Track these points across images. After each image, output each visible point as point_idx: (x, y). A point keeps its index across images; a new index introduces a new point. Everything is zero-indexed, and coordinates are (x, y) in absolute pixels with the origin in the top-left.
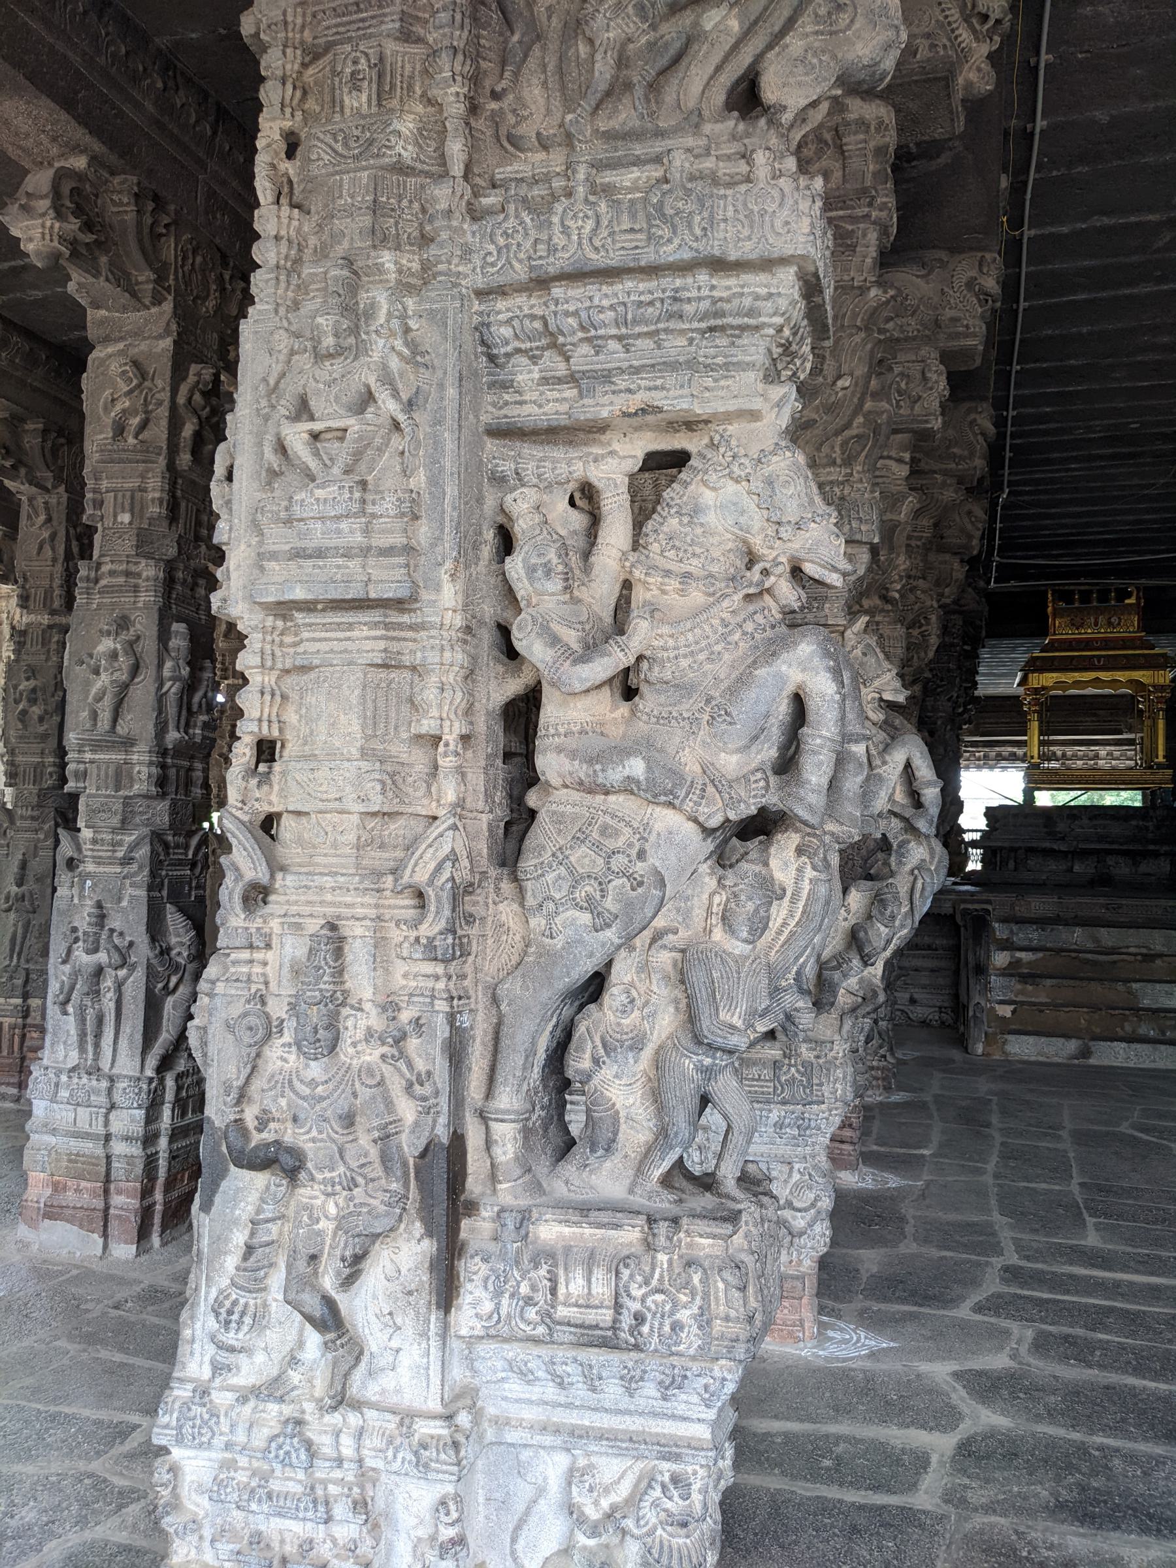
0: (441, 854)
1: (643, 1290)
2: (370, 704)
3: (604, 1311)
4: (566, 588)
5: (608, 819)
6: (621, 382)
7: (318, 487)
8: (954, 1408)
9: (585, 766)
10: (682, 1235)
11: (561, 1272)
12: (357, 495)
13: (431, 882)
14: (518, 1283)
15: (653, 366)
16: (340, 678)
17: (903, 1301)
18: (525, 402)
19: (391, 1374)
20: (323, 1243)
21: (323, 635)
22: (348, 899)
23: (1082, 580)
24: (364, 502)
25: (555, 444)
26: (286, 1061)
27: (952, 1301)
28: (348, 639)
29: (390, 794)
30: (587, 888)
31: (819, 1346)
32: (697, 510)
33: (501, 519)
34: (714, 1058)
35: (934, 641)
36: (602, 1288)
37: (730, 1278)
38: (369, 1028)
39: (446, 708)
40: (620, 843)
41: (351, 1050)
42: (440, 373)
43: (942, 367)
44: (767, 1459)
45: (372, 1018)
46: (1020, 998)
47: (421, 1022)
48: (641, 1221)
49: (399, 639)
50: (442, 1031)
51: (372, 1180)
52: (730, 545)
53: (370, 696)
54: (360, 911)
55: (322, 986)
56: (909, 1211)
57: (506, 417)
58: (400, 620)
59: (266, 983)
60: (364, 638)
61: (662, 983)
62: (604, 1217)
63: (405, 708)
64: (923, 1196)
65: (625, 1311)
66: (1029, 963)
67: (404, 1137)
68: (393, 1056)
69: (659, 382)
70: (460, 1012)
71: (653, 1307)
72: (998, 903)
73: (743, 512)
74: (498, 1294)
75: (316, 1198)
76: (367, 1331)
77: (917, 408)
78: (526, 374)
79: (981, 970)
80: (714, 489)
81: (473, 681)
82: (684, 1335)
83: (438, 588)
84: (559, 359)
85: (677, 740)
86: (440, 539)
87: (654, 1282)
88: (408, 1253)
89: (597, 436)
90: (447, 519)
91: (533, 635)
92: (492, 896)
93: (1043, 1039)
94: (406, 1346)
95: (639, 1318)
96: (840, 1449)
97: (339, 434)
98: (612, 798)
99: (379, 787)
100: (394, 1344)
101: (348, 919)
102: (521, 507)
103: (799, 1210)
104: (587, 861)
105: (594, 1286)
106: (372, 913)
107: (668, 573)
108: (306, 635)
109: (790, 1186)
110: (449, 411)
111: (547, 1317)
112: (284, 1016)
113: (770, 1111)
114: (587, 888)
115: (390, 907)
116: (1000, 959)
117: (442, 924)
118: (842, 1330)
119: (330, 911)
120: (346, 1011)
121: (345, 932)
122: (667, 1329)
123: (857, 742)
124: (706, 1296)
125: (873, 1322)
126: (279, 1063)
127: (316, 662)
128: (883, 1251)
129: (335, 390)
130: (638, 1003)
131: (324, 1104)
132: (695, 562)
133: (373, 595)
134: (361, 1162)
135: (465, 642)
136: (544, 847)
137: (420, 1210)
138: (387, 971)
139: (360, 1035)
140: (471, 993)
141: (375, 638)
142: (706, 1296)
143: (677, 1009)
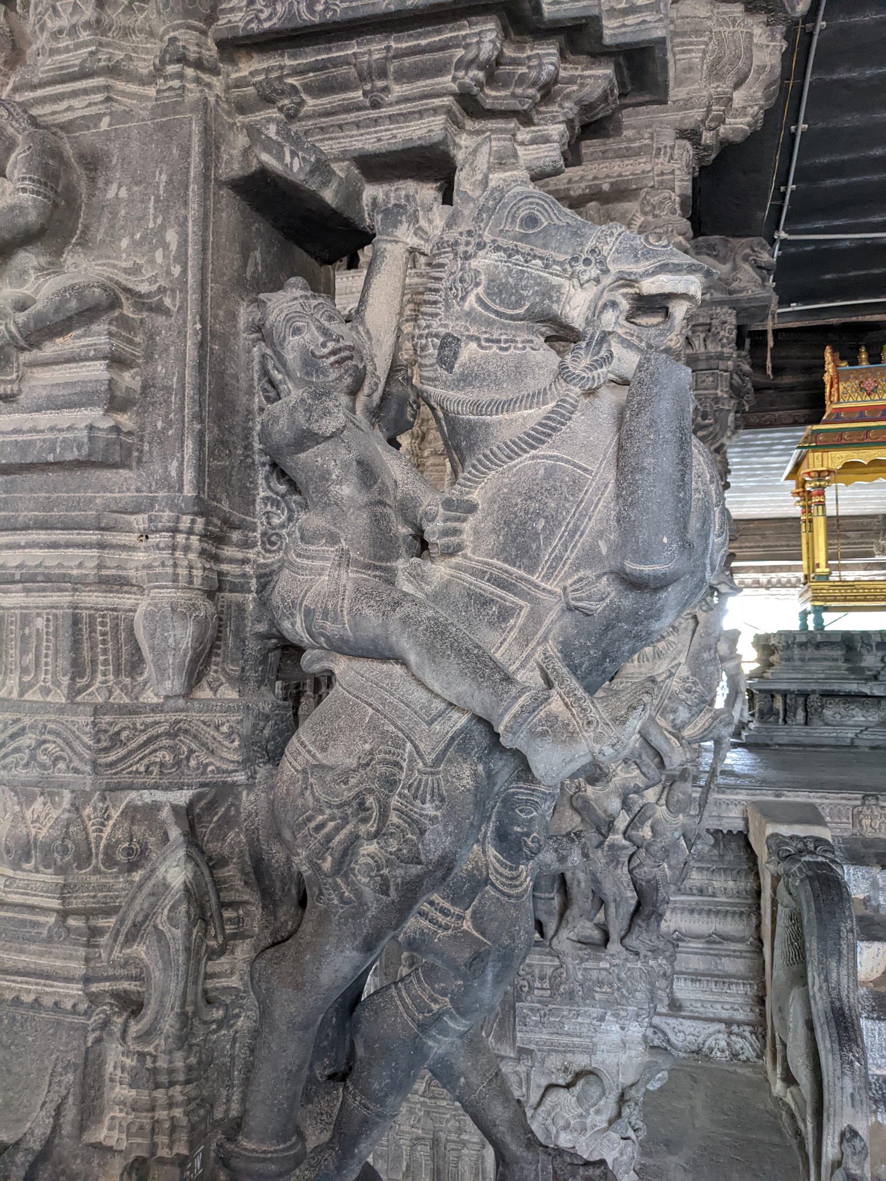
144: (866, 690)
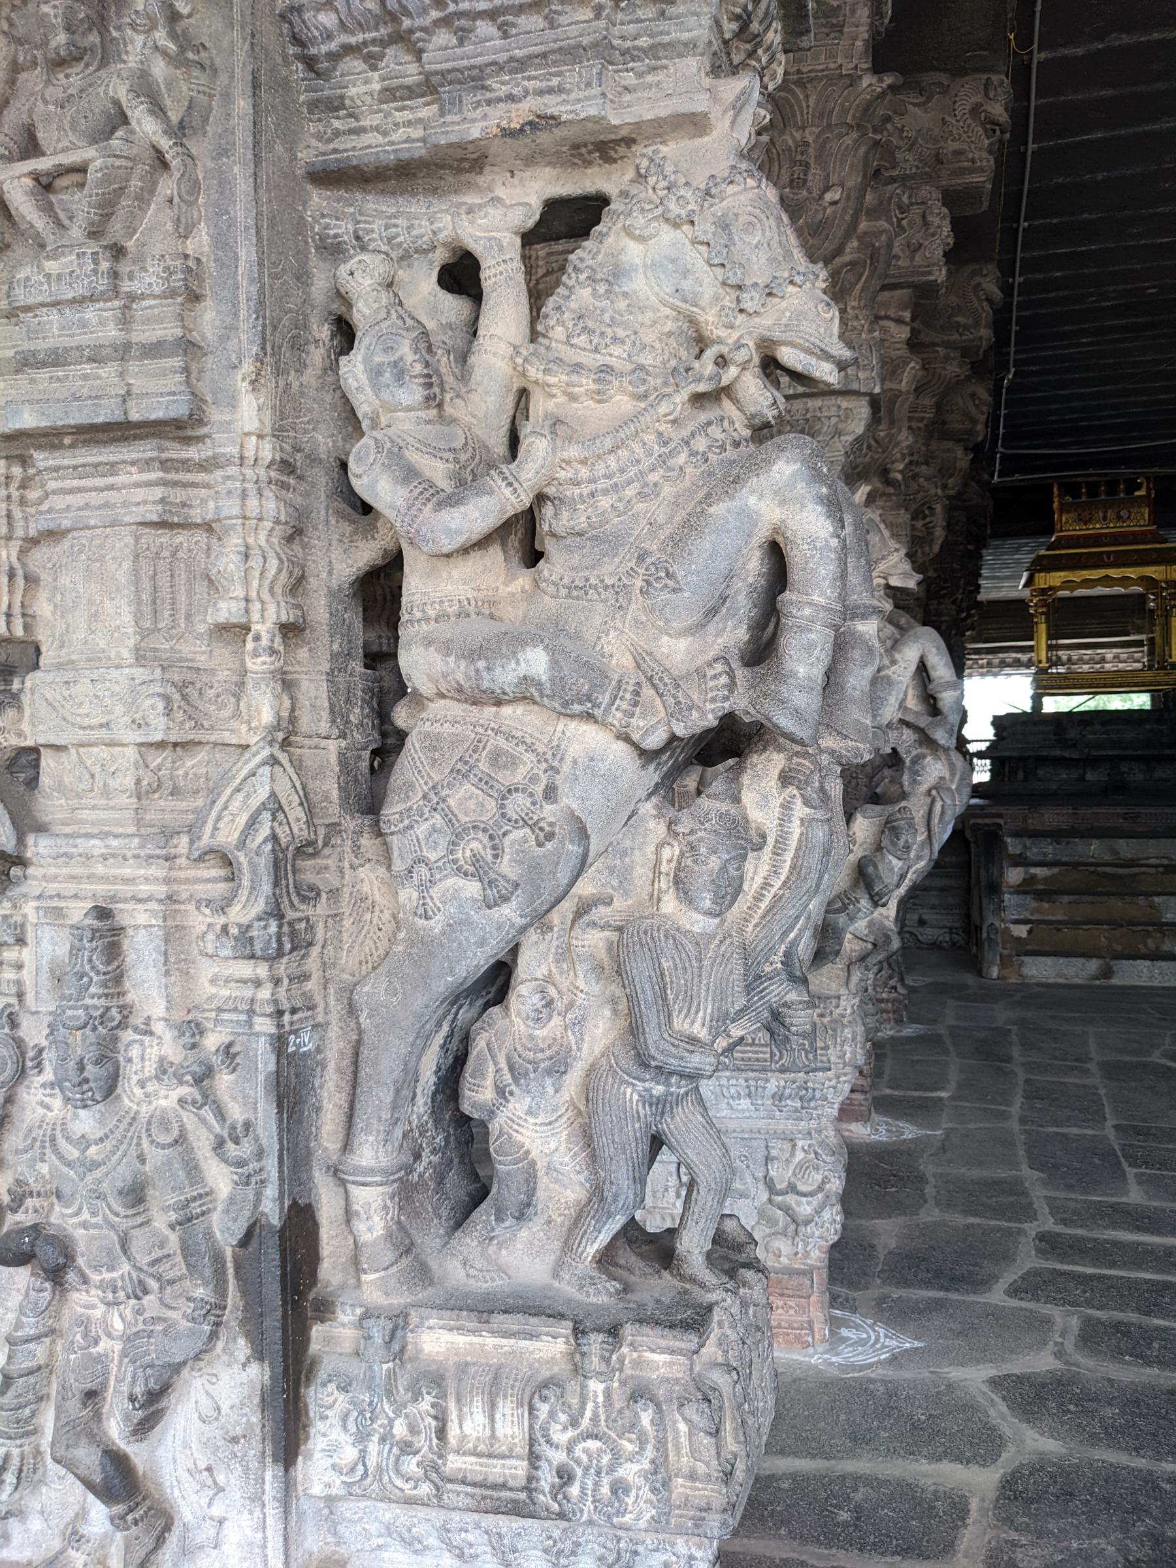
0: (255, 802)
1: (570, 1434)
2: (146, 584)
3: (514, 1462)
4: (428, 399)
5: (501, 742)
6: (499, 86)
7: (48, 258)
8: (993, 1429)
9: (463, 664)
10: (625, 1350)
11: (452, 1405)
12: (105, 265)
13: (242, 844)
14: (391, 1423)
15: (544, 55)
16: (102, 546)
17: (926, 1284)
18: (363, 130)
19: (214, 1553)
20: (106, 1373)
21: (77, 483)
22: (127, 871)
23: (1091, 471)
24: (115, 275)
25: (413, 194)
26: (47, 1107)
27: (983, 1282)
28: (111, 488)
29: (179, 716)
30: (474, 845)
31: (833, 1350)
32: (617, 273)
33: (336, 307)
34: (667, 1084)
35: (939, 533)
36: (510, 1427)
37: (696, 1418)
38: (161, 1060)
39: (255, 583)
40: (519, 776)
41: (138, 1092)
42: (223, 78)
43: (945, 210)
44: (772, 1514)
45: (166, 1045)
46: (1036, 917)
47: (233, 1050)
48: (565, 1328)
49: (185, 485)
50: (265, 1061)
51: (171, 1282)
52: (669, 326)
53: (146, 569)
54: (144, 889)
55: (88, 1001)
56: (928, 1167)
57: (335, 151)
58: (184, 455)
59: (20, 996)
60: (132, 484)
61: (592, 977)
62: (512, 1322)
63: (201, 588)
64: (944, 1149)
65: (543, 1463)
66: (1045, 880)
67: (216, 1218)
68: (194, 1102)
69: (555, 82)
70: (295, 1032)
71: (584, 1458)
72: (1010, 816)
73: (686, 273)
74: (362, 1437)
75: (93, 1307)
76: (177, 1493)
77: (918, 258)
78: (360, 84)
79: (994, 889)
80: (641, 239)
81: (305, 546)
82: (630, 1500)
83: (233, 403)
84: (408, 58)
85: (598, 619)
86: (233, 328)
87: (585, 1422)
88: (229, 1384)
89: (471, 177)
90: (243, 297)
91: (377, 468)
92: (349, 857)
93: (1062, 960)
94: (232, 1515)
95: (565, 1476)
96: (858, 1496)
97: (77, 177)
98: (507, 710)
99: (161, 705)
100: (217, 1511)
101: (126, 900)
102: (362, 279)
103: (805, 1195)
104: (471, 804)
105: (499, 1425)
106: (161, 890)
107: (577, 368)
108: (52, 485)
109: (792, 1166)
110: (239, 133)
111: (432, 1470)
112: (45, 1043)
113: (767, 1080)
114: (474, 845)
115: (187, 881)
116: (1014, 876)
117: (260, 906)
118: (857, 1327)
119: (102, 888)
120: (128, 1035)
121: (123, 920)
122: (605, 1490)
123: (864, 617)
124: (661, 1445)
125: (895, 1315)
126: (41, 1111)
127: (66, 524)
128: (901, 1220)
129: (71, 111)
130: (559, 1005)
131: (98, 1173)
132: (617, 350)
133: (135, 416)
134: (154, 1256)
135: (284, 486)
136: (412, 786)
137: (243, 1322)
138: (186, 974)
139: (150, 1068)
140: (318, 999)
141: (149, 484)
142: (661, 1445)
143: (615, 1011)
144: (1067, 755)
